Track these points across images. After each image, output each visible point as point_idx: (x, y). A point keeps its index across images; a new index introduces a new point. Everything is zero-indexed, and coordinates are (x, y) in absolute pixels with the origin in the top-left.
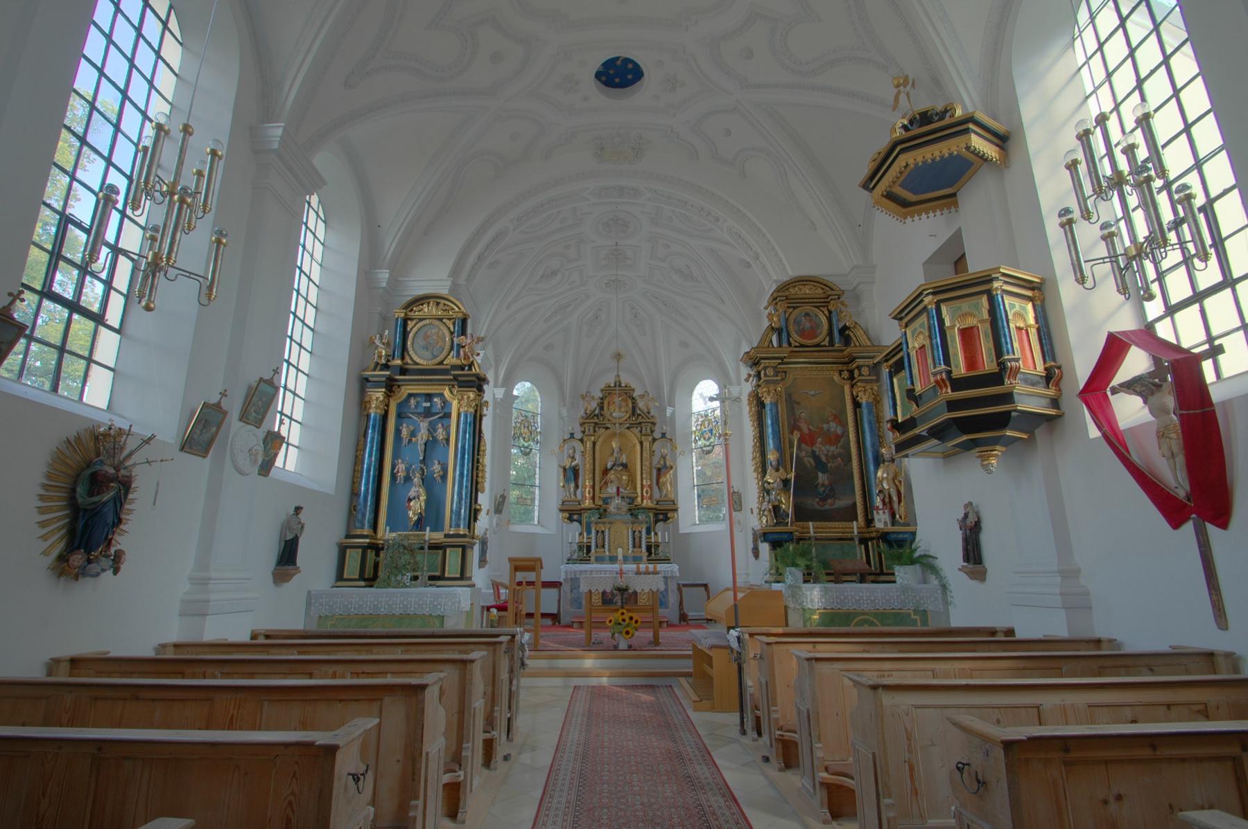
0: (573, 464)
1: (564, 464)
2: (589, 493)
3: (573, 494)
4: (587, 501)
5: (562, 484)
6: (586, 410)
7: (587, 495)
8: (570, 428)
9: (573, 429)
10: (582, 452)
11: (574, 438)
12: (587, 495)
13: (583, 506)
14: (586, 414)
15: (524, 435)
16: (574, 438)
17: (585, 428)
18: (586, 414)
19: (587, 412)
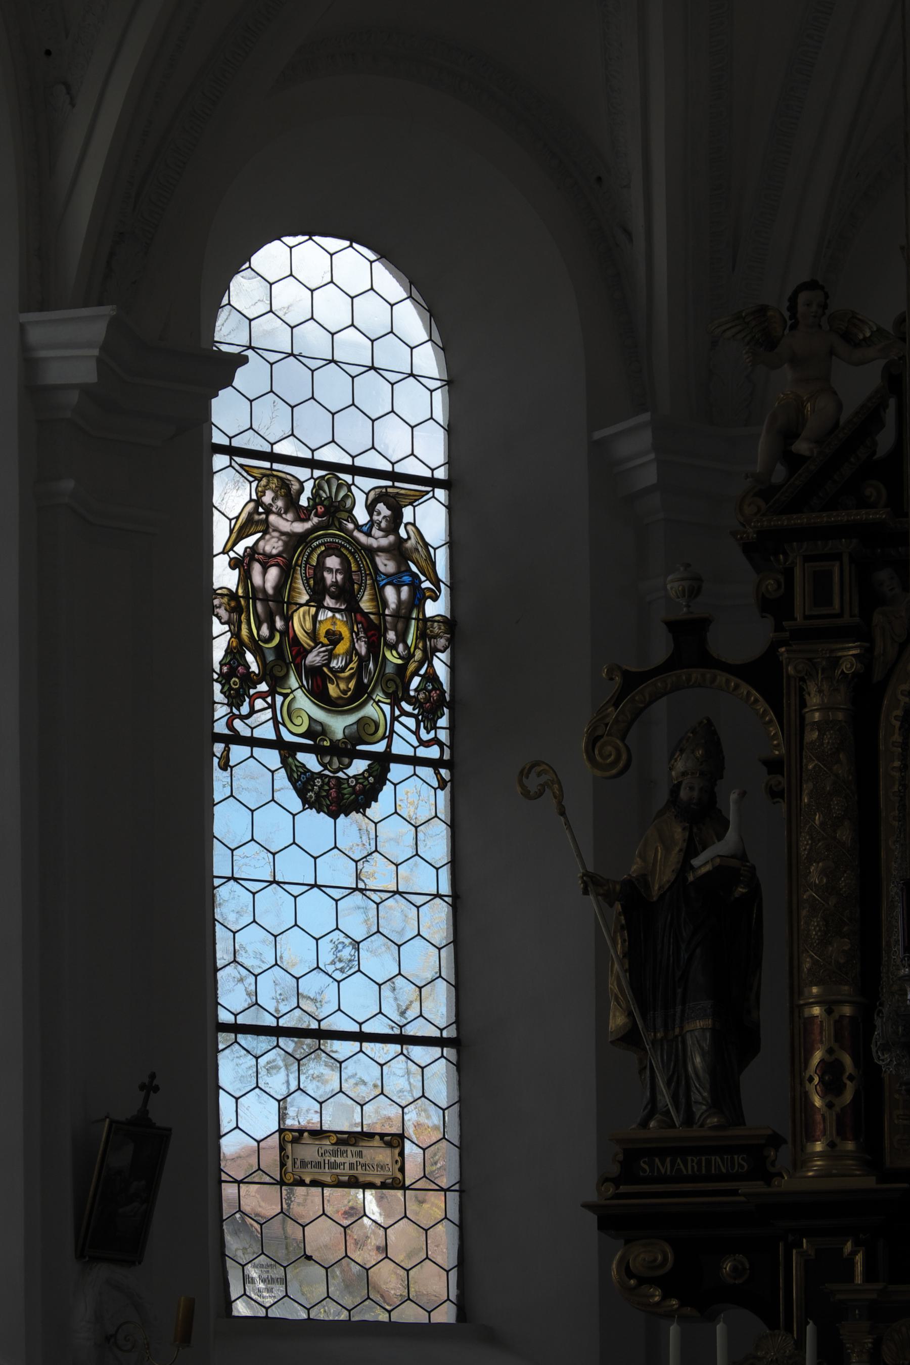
0: (702, 862)
1: (635, 868)
2: (832, 1087)
3: (700, 1095)
4: (819, 1147)
5: (617, 1021)
6: (789, 434)
7: (818, 1102)
8: (673, 585)
9: (694, 591)
10: (774, 766)
11: (707, 661)
12: (818, 1102)
13: (785, 1183)
14: (793, 461)
15: (314, 658)
16: (707, 661)
17: (789, 573)
18: (793, 461)
19: (802, 447)
